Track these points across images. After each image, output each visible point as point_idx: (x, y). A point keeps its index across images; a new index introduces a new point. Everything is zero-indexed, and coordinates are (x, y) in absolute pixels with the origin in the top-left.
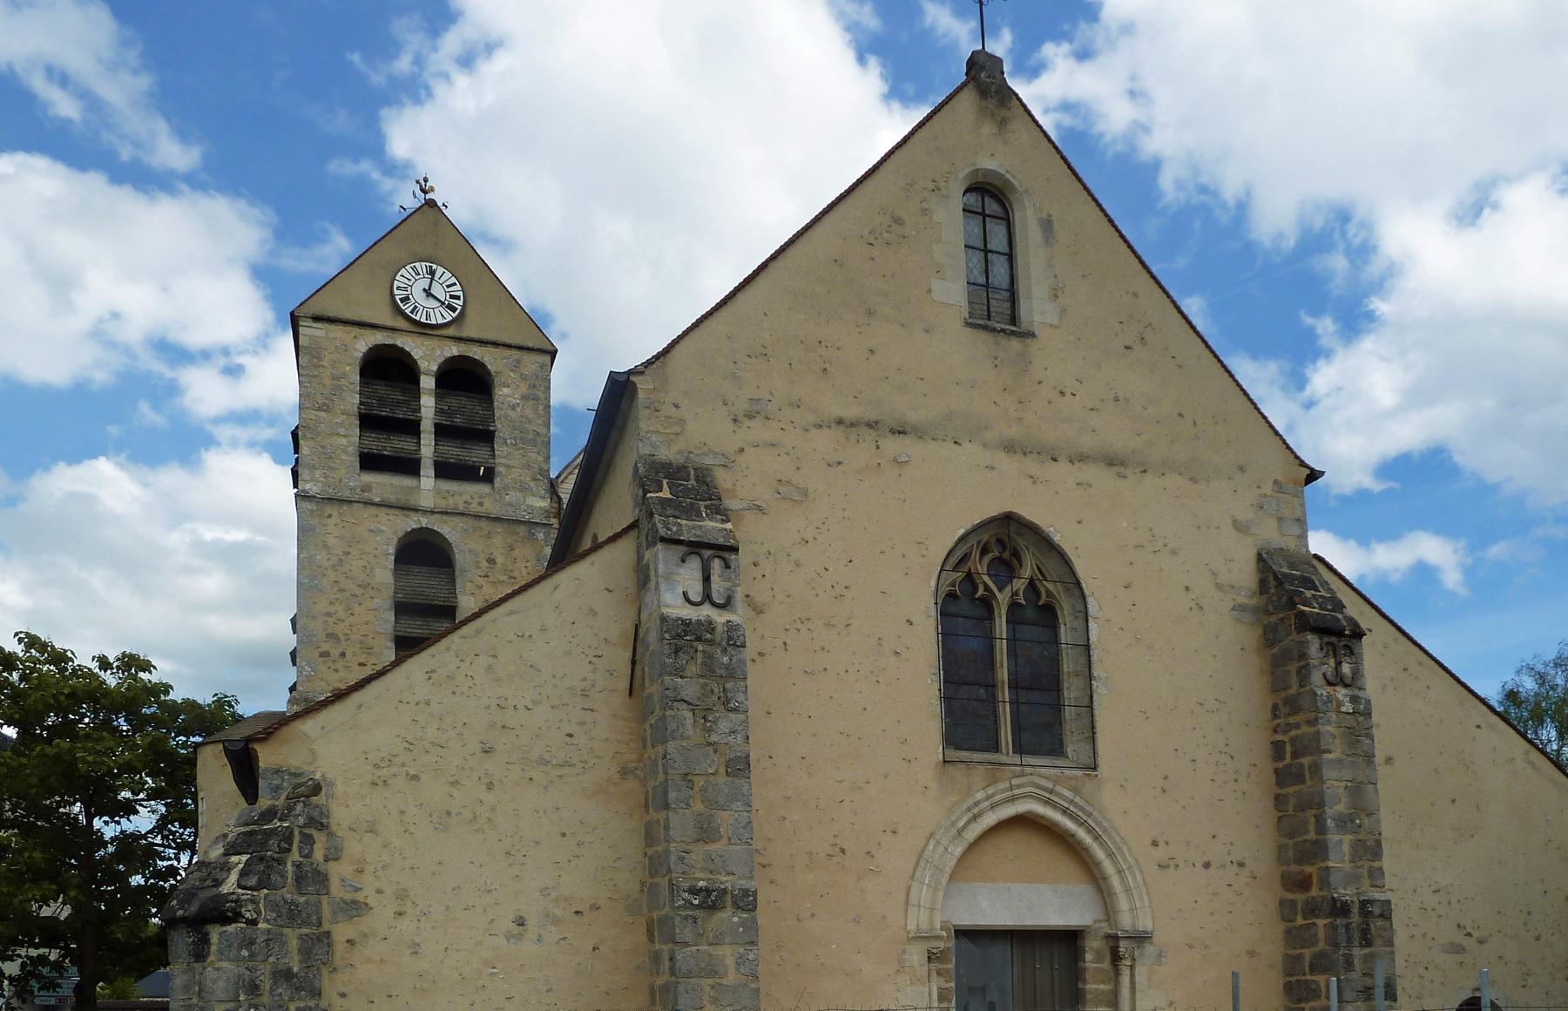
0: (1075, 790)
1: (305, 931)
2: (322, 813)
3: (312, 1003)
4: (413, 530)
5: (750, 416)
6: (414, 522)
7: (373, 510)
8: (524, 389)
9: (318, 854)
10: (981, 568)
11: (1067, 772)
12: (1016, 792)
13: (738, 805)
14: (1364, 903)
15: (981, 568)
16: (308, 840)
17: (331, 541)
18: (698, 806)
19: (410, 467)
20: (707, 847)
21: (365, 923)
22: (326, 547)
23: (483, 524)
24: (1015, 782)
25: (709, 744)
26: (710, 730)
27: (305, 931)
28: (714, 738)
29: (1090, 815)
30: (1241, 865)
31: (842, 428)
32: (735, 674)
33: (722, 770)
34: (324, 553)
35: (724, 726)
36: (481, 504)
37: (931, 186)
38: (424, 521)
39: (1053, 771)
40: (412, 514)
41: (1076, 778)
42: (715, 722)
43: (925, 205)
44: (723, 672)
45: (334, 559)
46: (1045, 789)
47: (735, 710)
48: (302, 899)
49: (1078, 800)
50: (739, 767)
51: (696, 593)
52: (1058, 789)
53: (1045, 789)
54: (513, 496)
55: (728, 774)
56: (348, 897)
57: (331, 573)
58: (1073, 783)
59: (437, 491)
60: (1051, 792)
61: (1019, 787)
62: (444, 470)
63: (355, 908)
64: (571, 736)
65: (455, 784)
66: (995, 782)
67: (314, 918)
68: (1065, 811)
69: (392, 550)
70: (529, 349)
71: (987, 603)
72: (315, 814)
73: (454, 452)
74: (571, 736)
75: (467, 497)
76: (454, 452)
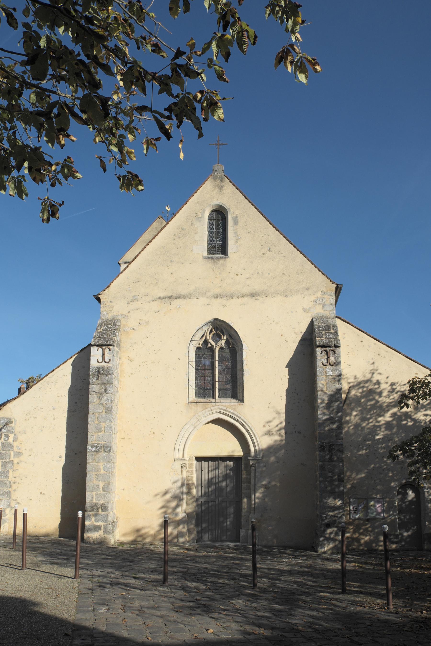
0: (235, 410)
1: (4, 460)
2: (12, 429)
3: (6, 479)
5: (132, 301)
9: (11, 440)
10: (210, 338)
11: (232, 404)
12: (213, 411)
13: (108, 421)
14: (330, 446)
15: (210, 338)
16: (8, 436)
18: (96, 422)
20: (98, 434)
21: (22, 458)
24: (212, 408)
25: (101, 404)
26: (101, 400)
27: (4, 460)
28: (102, 402)
29: (240, 418)
30: (299, 433)
31: (160, 300)
32: (109, 382)
33: (104, 411)
35: (105, 398)
37: (195, 215)
39: (227, 404)
41: (235, 406)
42: (103, 397)
43: (193, 222)
44: (106, 382)
46: (224, 410)
47: (108, 393)
48: (4, 452)
49: (235, 413)
50: (109, 410)
51: (100, 360)
52: (228, 409)
53: (224, 410)
55: (105, 412)
56: (18, 451)
58: (234, 408)
60: (226, 411)
61: (214, 410)
63: (19, 454)
64: (76, 403)
65: (45, 418)
66: (206, 408)
67: (8, 457)
68: (231, 417)
71: (212, 350)
72: (10, 429)
74: (76, 403)
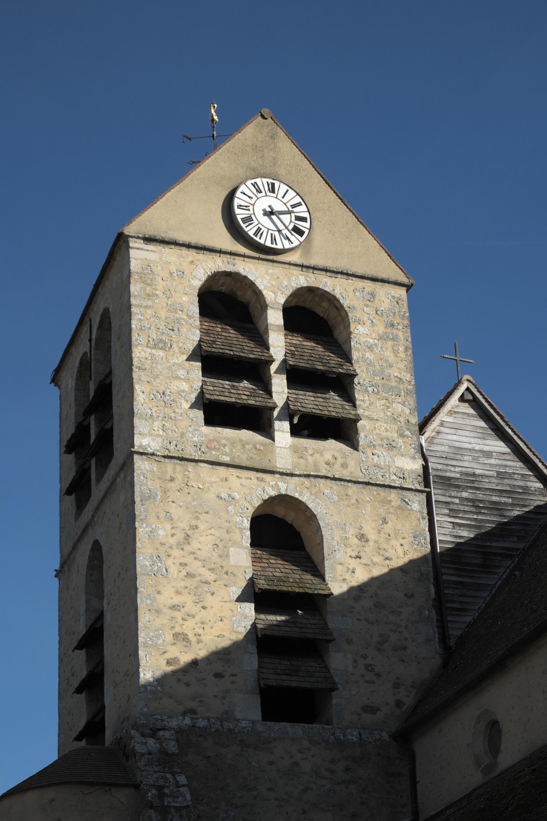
4: (272, 499)
6: (273, 487)
7: (221, 470)
8: (381, 329)
17: (174, 510)
19: (256, 420)
22: (169, 518)
23: (353, 489)
34: (168, 526)
36: (344, 466)
38: (285, 487)
40: (268, 477)
45: (180, 536)
54: (382, 457)
57: (175, 552)
59: (295, 449)
62: (309, 426)
69: (247, 524)
70: (383, 281)
73: (310, 402)
75: (328, 456)
76: (310, 402)
